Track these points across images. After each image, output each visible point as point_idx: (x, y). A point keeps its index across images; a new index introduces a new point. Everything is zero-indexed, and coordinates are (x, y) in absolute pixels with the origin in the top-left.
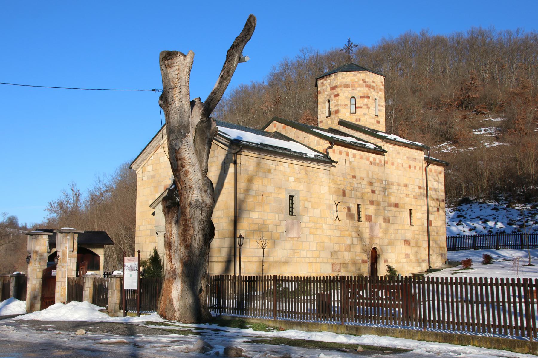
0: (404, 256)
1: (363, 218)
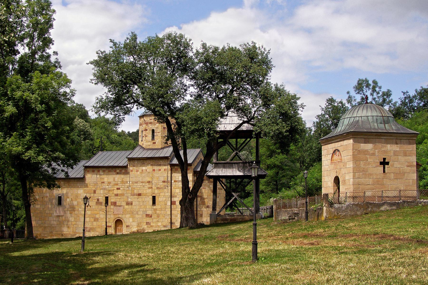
1: (109, 204)
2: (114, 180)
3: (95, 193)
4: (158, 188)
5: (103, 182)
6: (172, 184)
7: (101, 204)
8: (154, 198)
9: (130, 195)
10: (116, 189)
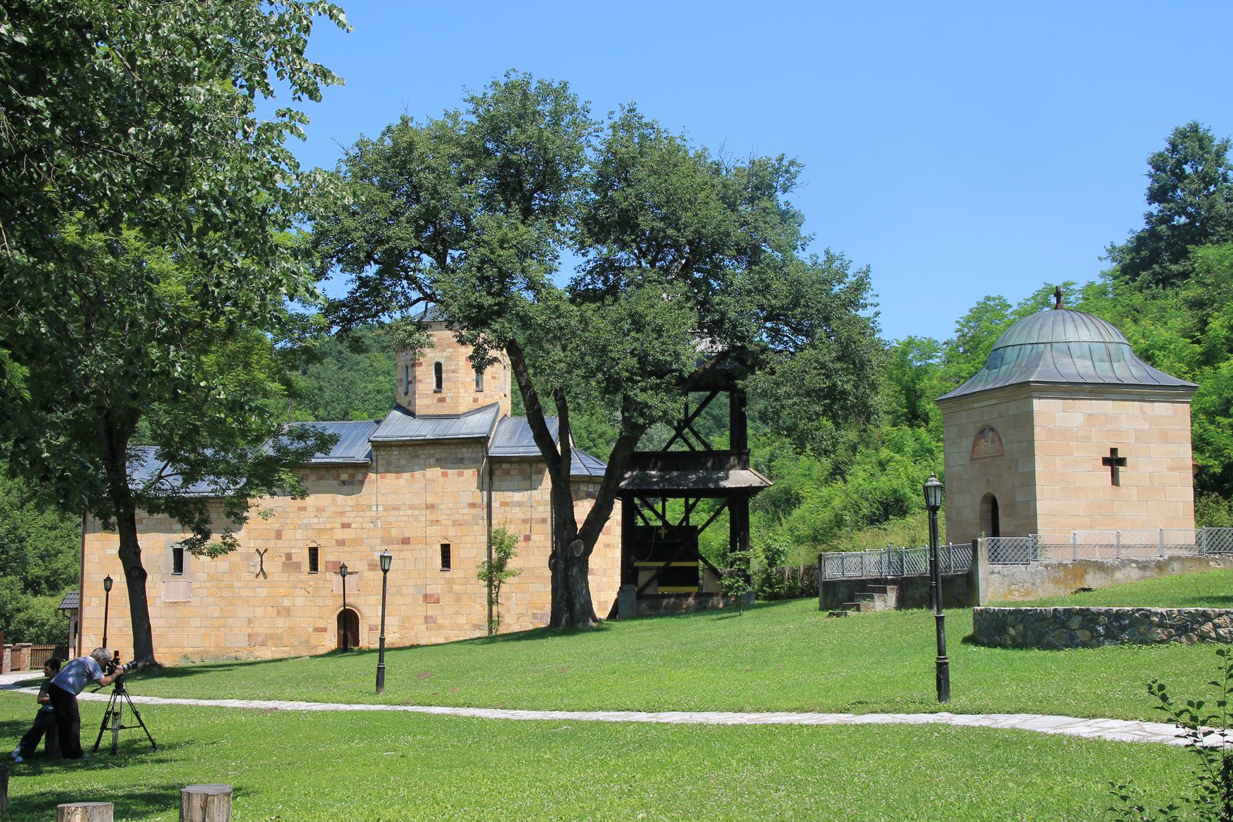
0: (422, 620)
1: (321, 566)
2: (334, 502)
3: (280, 539)
4: (455, 523)
5: (304, 509)
6: (494, 510)
7: (297, 567)
8: (446, 549)
9: (379, 541)
10: (339, 526)
